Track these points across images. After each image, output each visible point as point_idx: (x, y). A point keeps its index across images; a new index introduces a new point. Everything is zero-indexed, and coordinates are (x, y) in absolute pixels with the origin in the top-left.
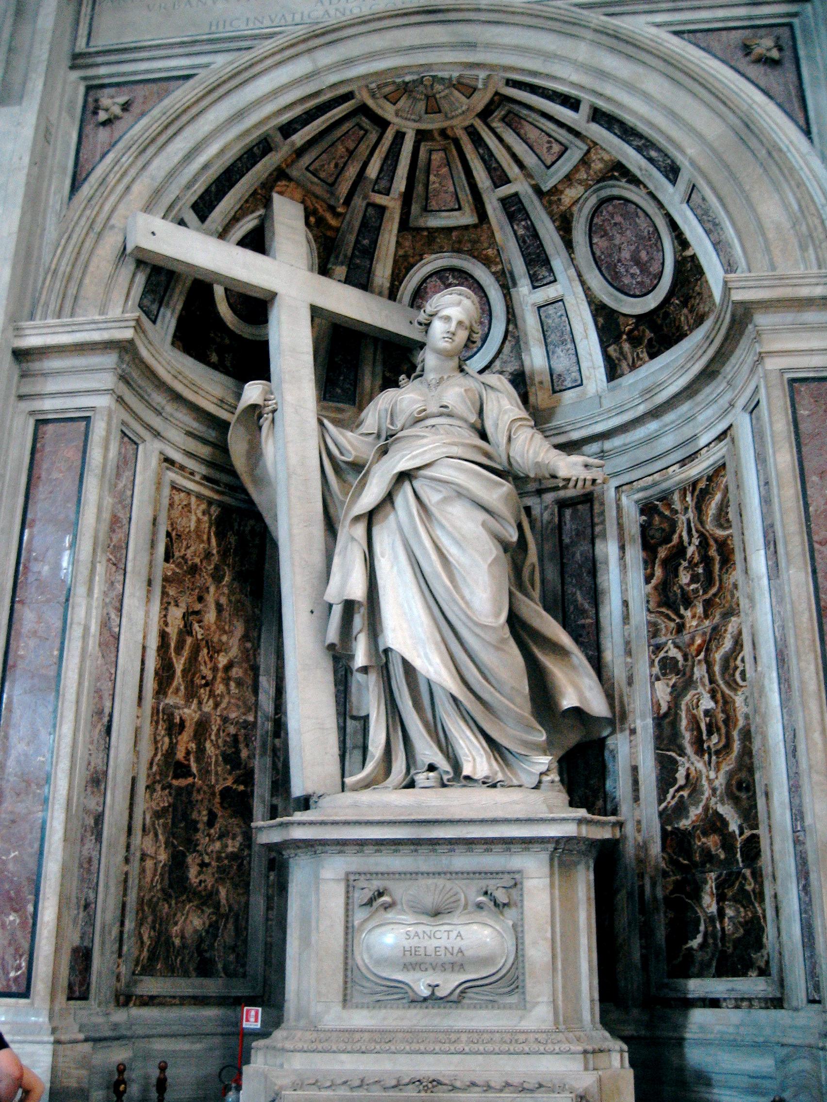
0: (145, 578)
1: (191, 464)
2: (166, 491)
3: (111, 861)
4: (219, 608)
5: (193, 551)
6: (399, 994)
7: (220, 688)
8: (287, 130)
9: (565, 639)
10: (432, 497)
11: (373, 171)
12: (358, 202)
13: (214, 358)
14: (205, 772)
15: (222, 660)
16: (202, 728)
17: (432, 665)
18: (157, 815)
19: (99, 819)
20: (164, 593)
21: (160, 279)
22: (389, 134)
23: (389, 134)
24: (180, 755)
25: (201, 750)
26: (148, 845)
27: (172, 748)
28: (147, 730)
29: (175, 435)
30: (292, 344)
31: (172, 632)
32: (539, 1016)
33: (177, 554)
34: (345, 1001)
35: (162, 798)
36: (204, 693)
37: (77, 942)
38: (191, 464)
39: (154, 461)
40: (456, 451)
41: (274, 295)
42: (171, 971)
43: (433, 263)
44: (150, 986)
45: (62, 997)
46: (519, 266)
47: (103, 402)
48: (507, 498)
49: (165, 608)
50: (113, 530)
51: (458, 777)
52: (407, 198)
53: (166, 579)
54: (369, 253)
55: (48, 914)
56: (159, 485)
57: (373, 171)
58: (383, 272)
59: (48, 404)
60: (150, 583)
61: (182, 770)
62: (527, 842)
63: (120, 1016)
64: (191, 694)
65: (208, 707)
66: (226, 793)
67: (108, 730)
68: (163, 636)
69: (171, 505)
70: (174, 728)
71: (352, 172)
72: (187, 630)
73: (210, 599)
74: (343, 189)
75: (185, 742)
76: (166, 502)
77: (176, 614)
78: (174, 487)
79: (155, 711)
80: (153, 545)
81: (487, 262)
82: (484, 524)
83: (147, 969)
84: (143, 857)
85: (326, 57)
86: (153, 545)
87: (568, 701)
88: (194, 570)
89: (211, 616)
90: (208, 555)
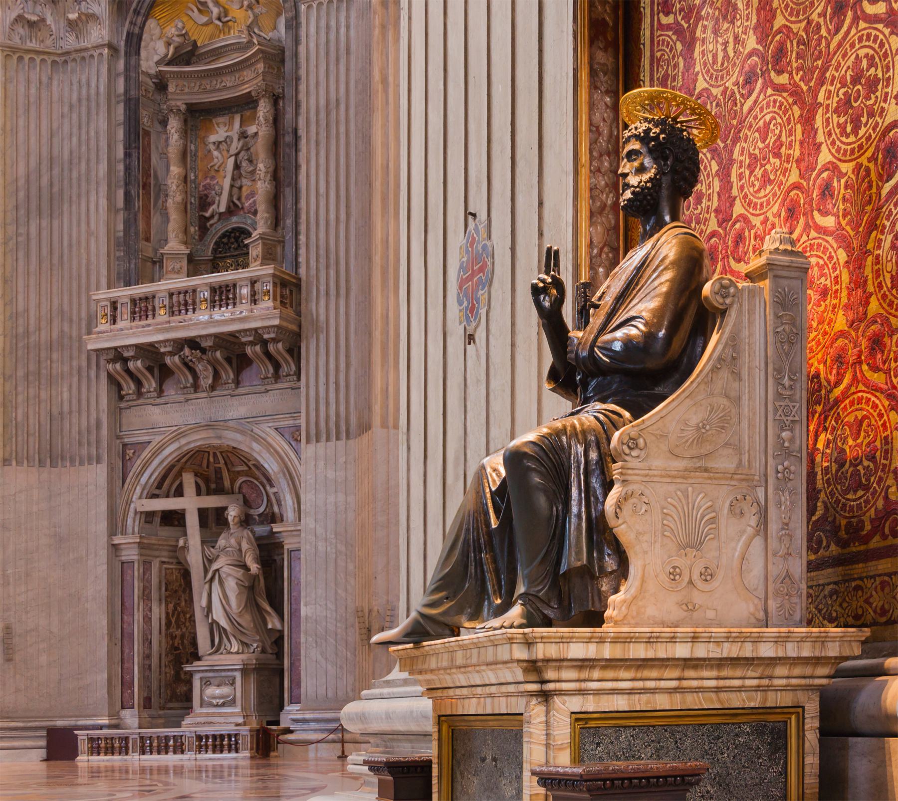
0: (158, 598)
1: (171, 560)
2: (163, 572)
3: (154, 675)
4: (186, 601)
5: (175, 586)
6: (211, 705)
7: (188, 624)
8: (178, 461)
9: (269, 609)
10: (223, 576)
11: (211, 460)
12: (212, 468)
13: (176, 523)
14: (184, 648)
15: (188, 616)
16: (183, 636)
17: (224, 623)
18: (169, 662)
19: (150, 666)
20: (166, 601)
21: (149, 516)
22: (211, 454)
23: (211, 454)
24: (176, 645)
25: (183, 643)
26: (167, 670)
27: (173, 644)
28: (164, 640)
29: (165, 553)
30: (192, 521)
31: (170, 611)
32: (238, 710)
33: (170, 588)
34: (201, 706)
35: (171, 657)
36: (182, 626)
37: (146, 695)
38: (171, 560)
39: (157, 565)
40: (229, 562)
41: (184, 510)
42: (177, 701)
43: (242, 479)
44: (170, 705)
45: (142, 709)
46: (265, 481)
47: (136, 557)
48: (243, 574)
49: (167, 605)
50: (144, 590)
51: (230, 653)
52: (226, 463)
53: (166, 597)
54: (219, 479)
55: (136, 690)
56: (160, 571)
57: (211, 460)
58: (227, 483)
59: (124, 558)
60: (160, 600)
61: (177, 649)
62: (236, 670)
63: (161, 712)
64: (178, 627)
65: (184, 630)
66: (191, 653)
67: (151, 643)
68: (167, 614)
69: (166, 575)
70: (173, 638)
71: (205, 461)
72: (175, 609)
73: (183, 599)
74: (205, 465)
75: (177, 642)
76: (164, 575)
77: (171, 606)
78: (166, 569)
79: (166, 635)
80: (160, 589)
81: (257, 479)
82: (237, 583)
83: (170, 701)
84: (166, 673)
85: (183, 441)
86: (160, 589)
87: (270, 626)
88: (176, 591)
89: (183, 604)
90: (181, 585)
